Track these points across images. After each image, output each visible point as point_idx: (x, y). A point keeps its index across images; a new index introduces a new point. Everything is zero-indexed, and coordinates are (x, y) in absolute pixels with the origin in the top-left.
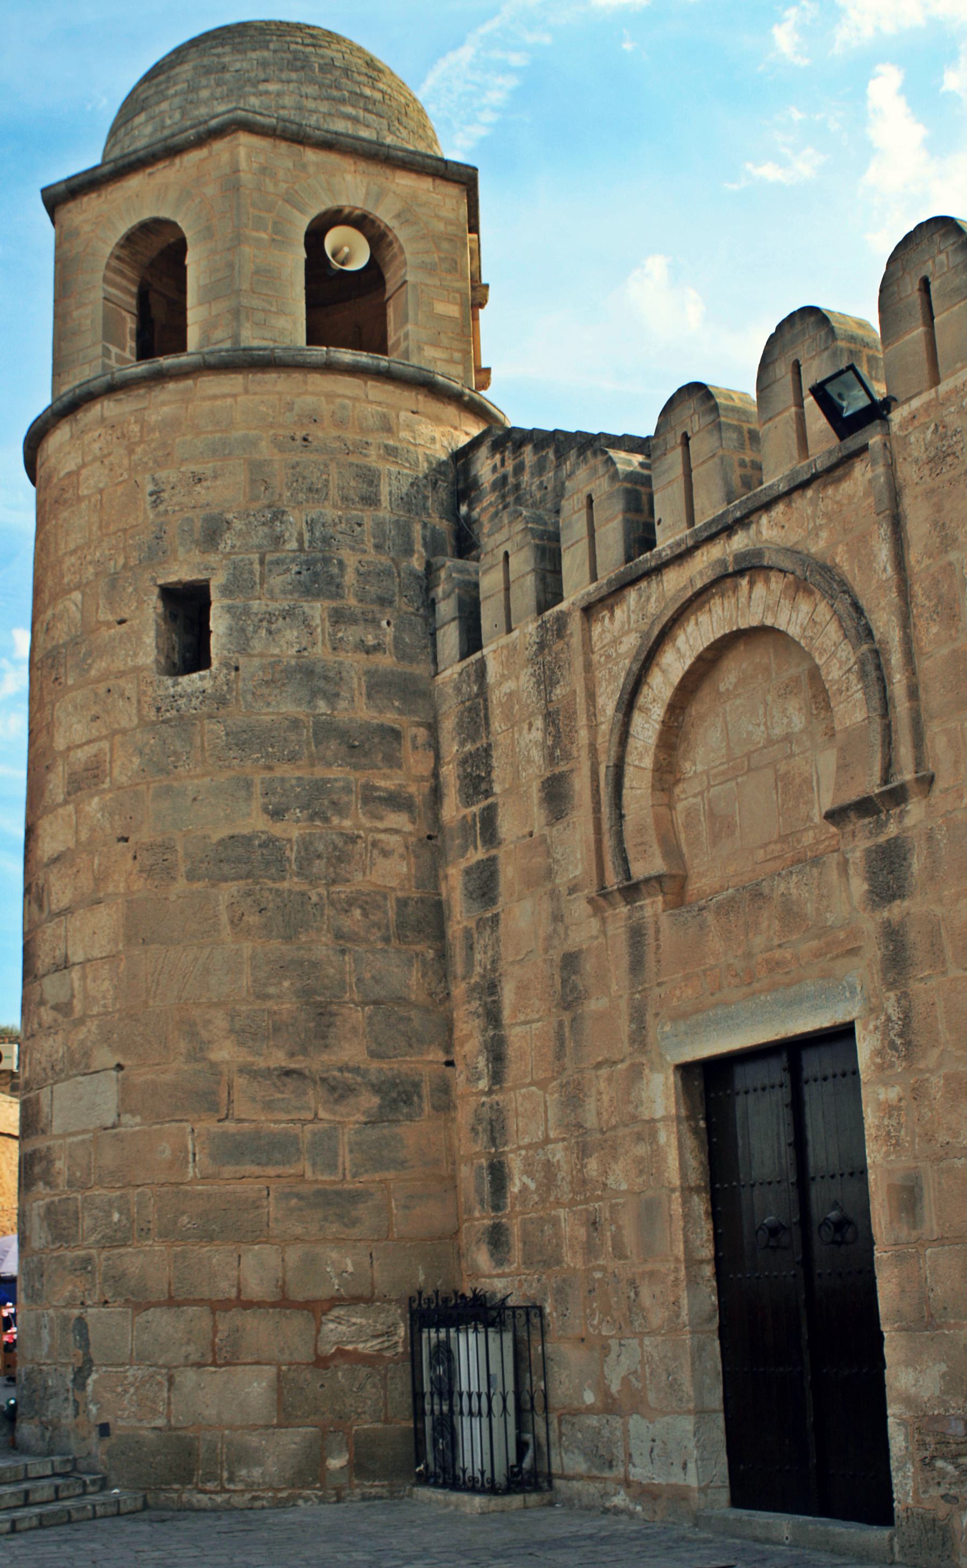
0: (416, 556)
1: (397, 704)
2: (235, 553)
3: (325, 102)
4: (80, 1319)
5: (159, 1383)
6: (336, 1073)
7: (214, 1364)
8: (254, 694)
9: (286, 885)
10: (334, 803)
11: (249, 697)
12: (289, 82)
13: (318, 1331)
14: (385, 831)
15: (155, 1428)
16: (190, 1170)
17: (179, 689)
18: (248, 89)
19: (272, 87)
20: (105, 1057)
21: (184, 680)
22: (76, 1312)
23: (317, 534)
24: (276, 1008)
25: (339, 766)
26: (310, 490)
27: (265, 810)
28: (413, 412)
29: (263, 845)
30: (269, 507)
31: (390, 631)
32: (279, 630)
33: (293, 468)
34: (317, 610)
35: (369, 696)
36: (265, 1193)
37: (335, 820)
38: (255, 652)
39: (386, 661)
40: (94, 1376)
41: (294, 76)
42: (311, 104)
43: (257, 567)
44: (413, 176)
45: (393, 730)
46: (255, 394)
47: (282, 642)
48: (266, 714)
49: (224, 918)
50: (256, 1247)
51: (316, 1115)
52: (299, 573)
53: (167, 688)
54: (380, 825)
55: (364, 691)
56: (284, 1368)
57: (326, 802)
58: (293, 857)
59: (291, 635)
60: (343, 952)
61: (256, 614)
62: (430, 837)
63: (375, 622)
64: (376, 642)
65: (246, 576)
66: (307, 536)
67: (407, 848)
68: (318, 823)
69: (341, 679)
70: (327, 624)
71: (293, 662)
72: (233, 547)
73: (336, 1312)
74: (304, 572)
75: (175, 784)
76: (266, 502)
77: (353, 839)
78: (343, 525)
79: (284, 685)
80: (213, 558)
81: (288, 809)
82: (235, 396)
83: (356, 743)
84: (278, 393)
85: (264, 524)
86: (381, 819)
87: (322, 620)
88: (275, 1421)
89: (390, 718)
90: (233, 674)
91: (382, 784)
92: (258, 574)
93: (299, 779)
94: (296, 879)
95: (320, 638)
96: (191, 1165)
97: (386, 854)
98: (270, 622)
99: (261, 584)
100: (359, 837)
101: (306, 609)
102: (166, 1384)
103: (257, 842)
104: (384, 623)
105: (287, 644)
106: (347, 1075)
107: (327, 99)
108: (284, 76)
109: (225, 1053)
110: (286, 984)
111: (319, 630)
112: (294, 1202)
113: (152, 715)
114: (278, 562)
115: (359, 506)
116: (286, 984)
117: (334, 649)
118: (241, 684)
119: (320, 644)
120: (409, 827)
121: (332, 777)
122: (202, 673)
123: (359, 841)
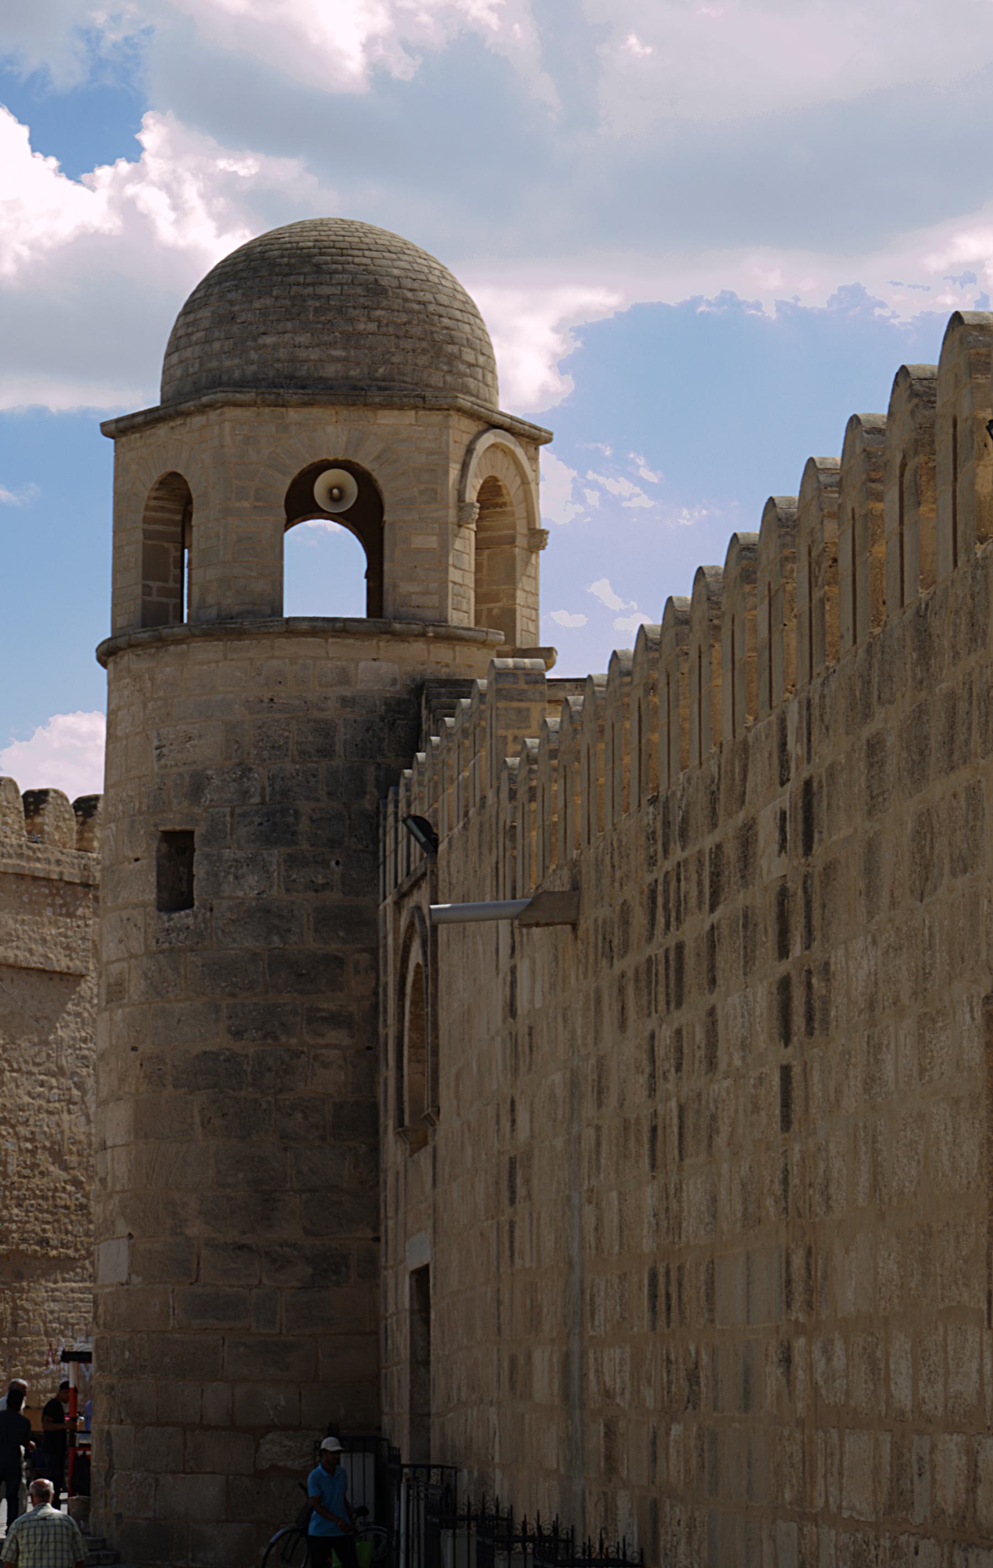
0: (368, 797)
1: (341, 934)
2: (214, 807)
3: (316, 349)
4: (108, 1432)
5: (150, 1484)
6: (277, 1248)
7: (184, 1472)
8: (223, 931)
9: (243, 1093)
10: (282, 1024)
11: (220, 933)
12: (284, 333)
13: (257, 1450)
14: (327, 1046)
15: (146, 1518)
16: (171, 1321)
17: (172, 923)
18: (250, 343)
19: (268, 340)
21: (176, 915)
22: (106, 1427)
23: (277, 787)
24: (233, 1195)
25: (289, 992)
26: (273, 747)
27: (230, 1031)
28: (374, 660)
29: (227, 1060)
30: (240, 764)
31: (338, 870)
32: (243, 876)
33: (260, 728)
34: (274, 856)
35: (316, 930)
36: (221, 1342)
37: (283, 1039)
38: (225, 895)
39: (334, 897)
40: (115, 1477)
41: (289, 325)
42: (302, 354)
43: (228, 818)
44: (396, 413)
45: (336, 957)
46: (232, 660)
47: (246, 887)
48: (232, 949)
49: (197, 1120)
50: (215, 1384)
51: (260, 1282)
52: (261, 824)
53: (164, 923)
54: (321, 1041)
55: (312, 926)
56: (231, 1477)
57: (276, 1023)
58: (249, 1070)
59: (252, 880)
60: (286, 1149)
61: (227, 861)
62: (369, 1048)
63: (325, 864)
64: (324, 881)
65: (220, 827)
66: (268, 790)
67: (345, 1059)
68: (269, 1041)
69: (293, 916)
70: (283, 868)
71: (254, 904)
72: (211, 801)
73: (269, 1437)
74: (265, 823)
75: (167, 1006)
76: (237, 761)
77: (296, 1054)
78: (300, 778)
79: (246, 923)
80: (197, 810)
81: (246, 1031)
82: (217, 662)
83: (304, 972)
84: (250, 659)
85: (234, 781)
86: (323, 1035)
87: (279, 865)
88: (224, 1517)
90: (208, 913)
91: (325, 1006)
92: (229, 826)
93: (255, 1004)
94: (250, 1089)
95: (276, 881)
96: (171, 1318)
97: (325, 1065)
98: (236, 868)
99: (231, 834)
100: (302, 1052)
101: (266, 856)
102: (154, 1485)
103: (222, 1058)
104: (333, 863)
105: (249, 887)
106: (286, 1249)
107: (318, 345)
108: (280, 327)
109: (195, 1229)
110: (241, 1175)
111: (276, 874)
112: (242, 1349)
113: (153, 947)
114: (244, 815)
115: (315, 759)
116: (241, 1175)
117: (288, 890)
118: (214, 923)
119: (275, 887)
120: (347, 1041)
121: (282, 1001)
122: (187, 911)
123: (303, 1056)
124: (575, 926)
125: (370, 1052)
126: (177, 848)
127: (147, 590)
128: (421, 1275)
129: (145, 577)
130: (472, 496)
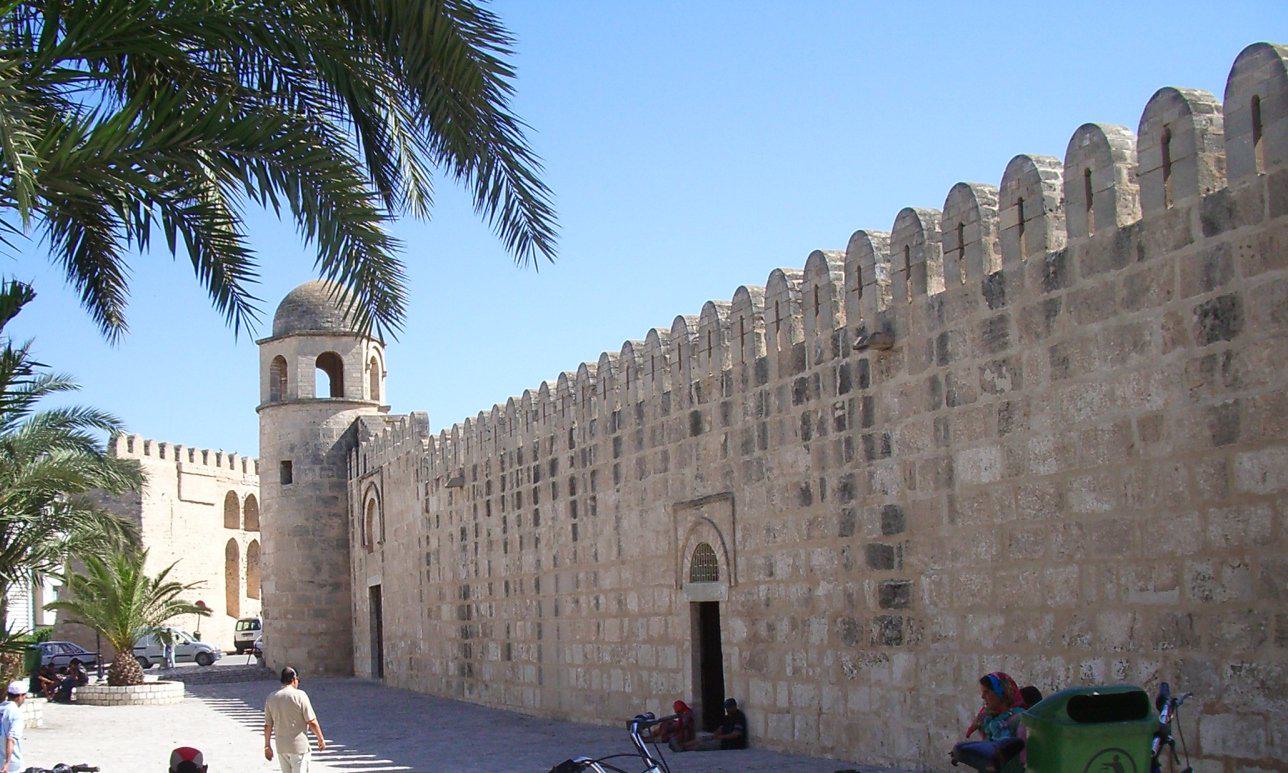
20: (272, 577)
34: (317, 468)
39: (335, 479)
89: (335, 494)
105: (310, 477)
124: (462, 487)
125: (346, 524)
126: (287, 466)
127: (272, 390)
128: (376, 591)
129: (271, 386)
130: (369, 362)
